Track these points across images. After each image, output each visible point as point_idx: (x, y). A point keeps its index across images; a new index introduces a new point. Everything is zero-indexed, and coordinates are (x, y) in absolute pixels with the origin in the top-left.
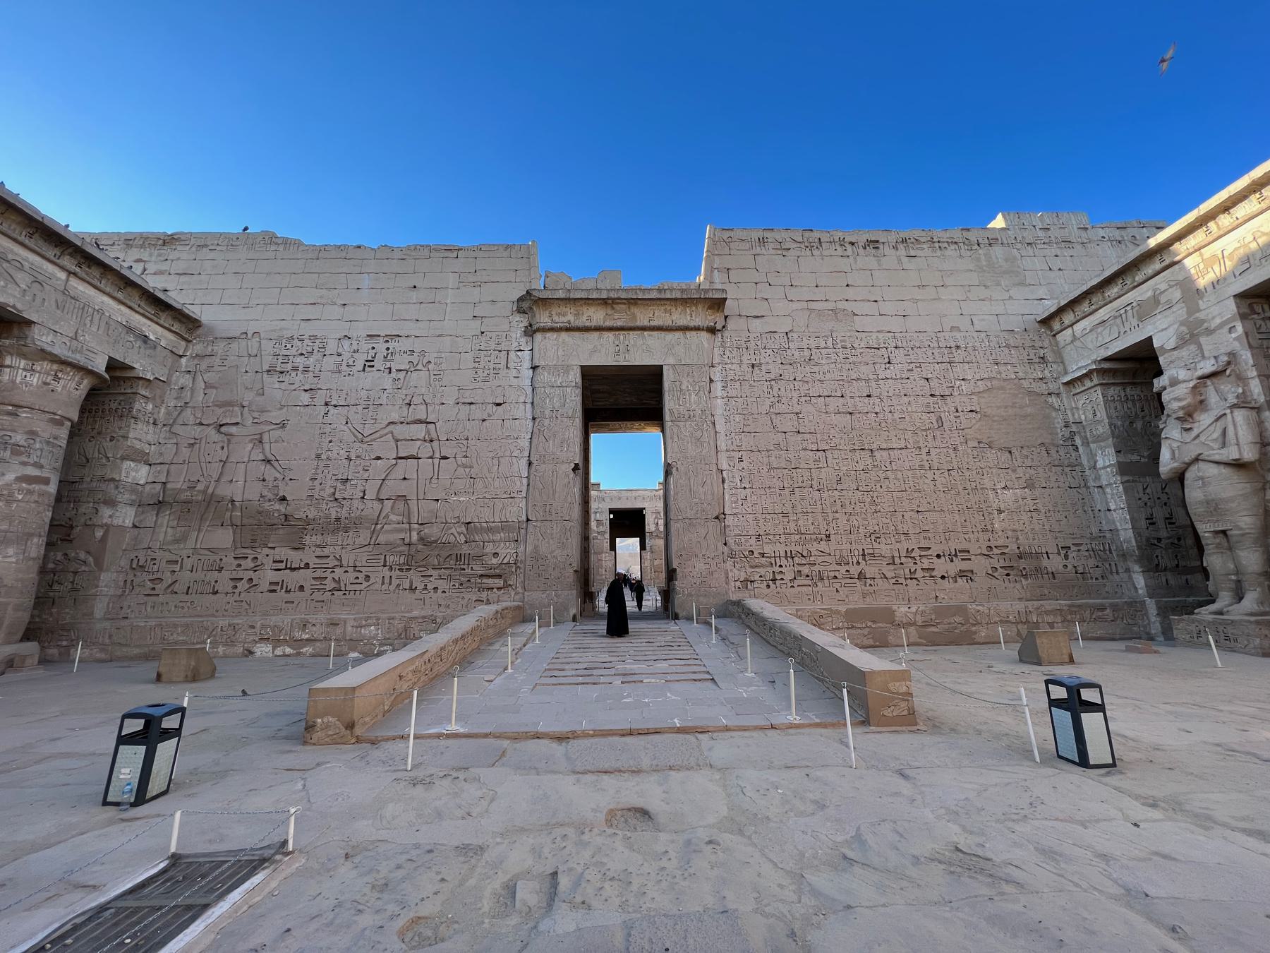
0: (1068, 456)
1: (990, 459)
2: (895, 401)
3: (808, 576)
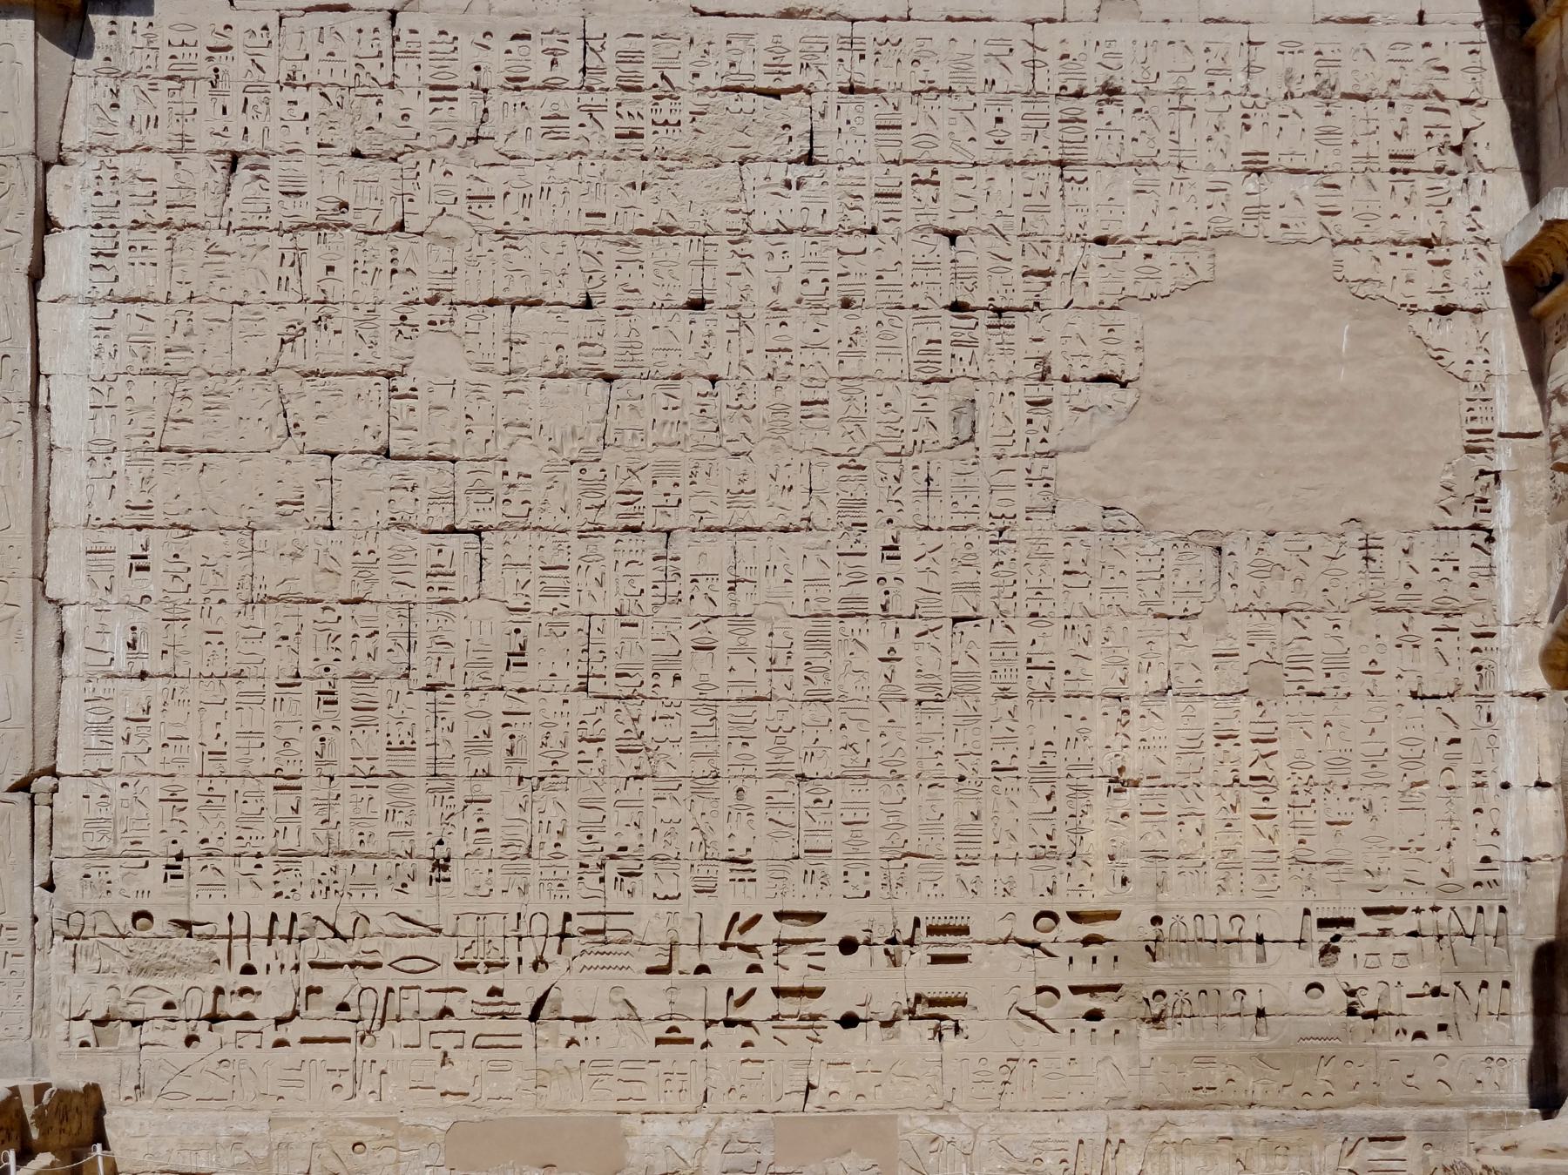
0: (1446, 568)
1: (1129, 581)
2: (799, 329)
3: (343, 1007)
